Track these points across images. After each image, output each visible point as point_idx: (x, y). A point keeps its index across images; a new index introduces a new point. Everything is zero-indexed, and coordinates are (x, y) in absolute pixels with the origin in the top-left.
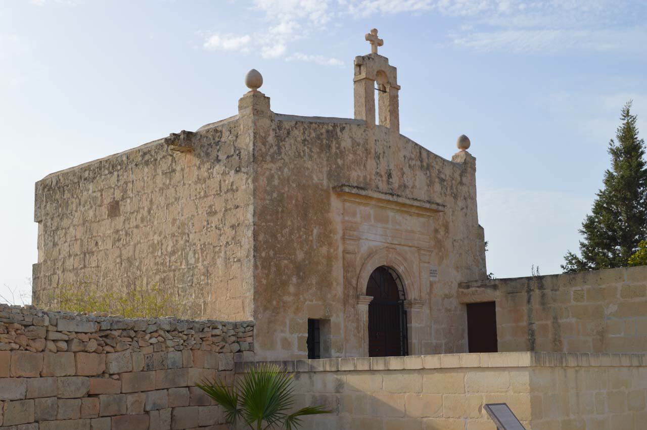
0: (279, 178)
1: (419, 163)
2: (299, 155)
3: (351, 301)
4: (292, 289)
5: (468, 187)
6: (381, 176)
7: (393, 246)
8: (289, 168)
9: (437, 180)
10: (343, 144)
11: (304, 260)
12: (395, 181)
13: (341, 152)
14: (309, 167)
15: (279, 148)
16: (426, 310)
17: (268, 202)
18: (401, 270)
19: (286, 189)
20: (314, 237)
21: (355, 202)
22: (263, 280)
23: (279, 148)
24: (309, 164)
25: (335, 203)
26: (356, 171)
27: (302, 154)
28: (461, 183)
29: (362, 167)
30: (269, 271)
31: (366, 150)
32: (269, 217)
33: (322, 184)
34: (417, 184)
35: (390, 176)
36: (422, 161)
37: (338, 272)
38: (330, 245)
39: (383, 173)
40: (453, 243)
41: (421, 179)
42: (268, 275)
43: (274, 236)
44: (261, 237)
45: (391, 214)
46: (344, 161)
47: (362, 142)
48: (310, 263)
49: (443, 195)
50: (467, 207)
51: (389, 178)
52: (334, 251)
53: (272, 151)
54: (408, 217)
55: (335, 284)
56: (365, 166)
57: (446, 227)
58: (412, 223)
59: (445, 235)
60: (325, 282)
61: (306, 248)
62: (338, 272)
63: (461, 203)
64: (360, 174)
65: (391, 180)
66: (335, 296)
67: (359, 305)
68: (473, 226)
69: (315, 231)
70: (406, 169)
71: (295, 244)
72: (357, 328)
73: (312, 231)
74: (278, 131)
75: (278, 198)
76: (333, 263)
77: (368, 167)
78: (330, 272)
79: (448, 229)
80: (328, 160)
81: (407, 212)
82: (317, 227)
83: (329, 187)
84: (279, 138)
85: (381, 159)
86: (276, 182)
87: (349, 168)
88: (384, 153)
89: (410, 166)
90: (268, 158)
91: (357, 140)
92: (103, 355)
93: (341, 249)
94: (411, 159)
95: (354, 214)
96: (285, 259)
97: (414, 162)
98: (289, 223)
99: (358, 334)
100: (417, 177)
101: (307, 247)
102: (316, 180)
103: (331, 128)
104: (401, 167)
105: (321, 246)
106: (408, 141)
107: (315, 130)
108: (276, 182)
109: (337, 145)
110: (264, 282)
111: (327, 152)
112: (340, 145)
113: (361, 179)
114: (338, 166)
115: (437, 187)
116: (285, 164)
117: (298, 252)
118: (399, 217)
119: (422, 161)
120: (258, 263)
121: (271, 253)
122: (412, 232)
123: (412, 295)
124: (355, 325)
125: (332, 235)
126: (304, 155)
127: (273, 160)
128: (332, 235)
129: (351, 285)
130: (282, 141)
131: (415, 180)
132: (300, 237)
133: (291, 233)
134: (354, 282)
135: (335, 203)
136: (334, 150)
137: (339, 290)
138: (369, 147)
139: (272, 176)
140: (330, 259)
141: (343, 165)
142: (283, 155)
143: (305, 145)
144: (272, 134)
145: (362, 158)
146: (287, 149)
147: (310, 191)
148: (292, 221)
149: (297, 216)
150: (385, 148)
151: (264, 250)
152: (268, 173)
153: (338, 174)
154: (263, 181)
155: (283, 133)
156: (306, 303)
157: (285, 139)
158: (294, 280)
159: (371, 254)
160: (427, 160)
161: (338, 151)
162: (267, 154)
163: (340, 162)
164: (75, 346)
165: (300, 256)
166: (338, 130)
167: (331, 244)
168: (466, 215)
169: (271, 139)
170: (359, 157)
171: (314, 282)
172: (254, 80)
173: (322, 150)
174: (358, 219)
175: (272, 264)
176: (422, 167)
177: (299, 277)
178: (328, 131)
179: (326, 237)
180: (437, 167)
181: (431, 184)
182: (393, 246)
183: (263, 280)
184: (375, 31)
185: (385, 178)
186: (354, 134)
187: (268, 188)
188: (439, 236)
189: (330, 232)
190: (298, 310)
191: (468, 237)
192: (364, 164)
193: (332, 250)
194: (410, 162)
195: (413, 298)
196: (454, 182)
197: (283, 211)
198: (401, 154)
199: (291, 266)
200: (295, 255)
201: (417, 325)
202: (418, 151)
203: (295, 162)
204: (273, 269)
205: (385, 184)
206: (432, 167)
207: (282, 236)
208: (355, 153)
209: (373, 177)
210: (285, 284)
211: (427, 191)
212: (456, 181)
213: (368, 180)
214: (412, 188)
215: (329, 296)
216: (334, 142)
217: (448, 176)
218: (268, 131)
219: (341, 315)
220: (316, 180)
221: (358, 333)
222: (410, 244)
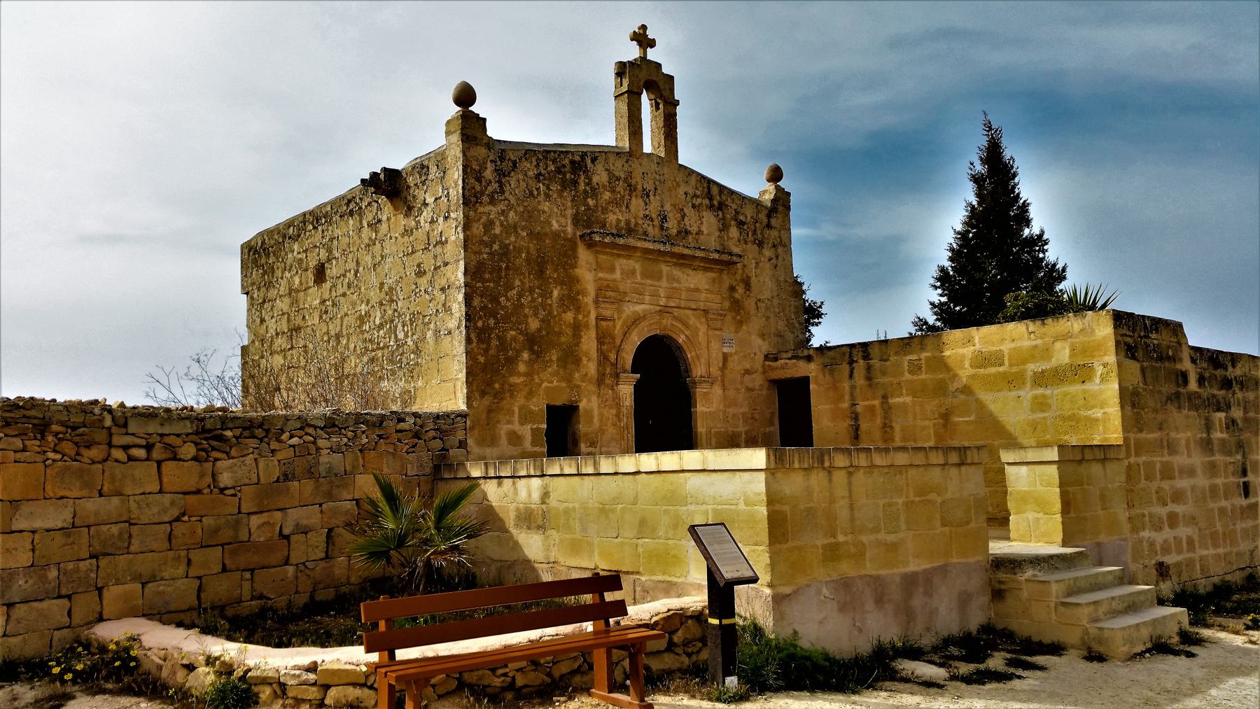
0: (502, 225)
1: (707, 202)
2: (531, 193)
4: (522, 368)
5: (779, 231)
6: (652, 220)
7: (670, 310)
8: (516, 212)
9: (733, 223)
10: (595, 179)
11: (539, 330)
12: (672, 225)
13: (593, 189)
14: (546, 209)
16: (717, 390)
17: (485, 256)
18: (681, 339)
19: (513, 239)
20: (554, 301)
21: (612, 254)
22: (479, 357)
24: (546, 206)
25: (584, 254)
26: (614, 213)
27: (536, 193)
28: (769, 226)
29: (624, 209)
30: (489, 344)
31: (630, 185)
32: (487, 276)
33: (564, 232)
34: (704, 229)
35: (664, 219)
36: (711, 199)
38: (578, 309)
39: (654, 216)
40: (756, 303)
41: (709, 223)
42: (486, 351)
43: (495, 300)
44: (476, 302)
45: (665, 269)
46: (597, 201)
47: (623, 176)
48: (548, 333)
49: (742, 242)
50: (777, 257)
51: (663, 222)
52: (583, 318)
54: (691, 272)
55: (585, 360)
56: (627, 207)
57: (747, 283)
58: (697, 280)
59: (745, 293)
60: (571, 358)
61: (542, 314)
62: (589, 343)
63: (768, 252)
64: (620, 218)
65: (666, 225)
66: (586, 375)
67: (620, 387)
68: (786, 281)
69: (556, 293)
70: (689, 211)
71: (527, 311)
72: (618, 415)
74: (499, 163)
75: (500, 251)
76: (583, 333)
77: (632, 208)
78: (577, 344)
79: (750, 286)
80: (573, 200)
82: (559, 288)
83: (574, 234)
84: (501, 174)
85: (652, 197)
86: (497, 230)
87: (605, 210)
88: (656, 189)
90: (485, 199)
91: (617, 174)
92: (209, 465)
93: (593, 316)
94: (695, 196)
95: (612, 270)
96: (511, 329)
97: (699, 201)
98: (517, 283)
99: (618, 423)
100: (704, 220)
101: (543, 313)
102: (555, 226)
103: (577, 158)
104: (681, 207)
105: (565, 312)
106: (691, 172)
107: (554, 161)
108: (497, 230)
109: (587, 181)
110: (482, 359)
111: (571, 191)
112: (591, 180)
113: (623, 224)
114: (589, 208)
115: (734, 232)
116: (510, 207)
117: (530, 320)
118: (677, 272)
119: (711, 199)
120: (473, 336)
121: (492, 322)
122: (697, 290)
123: (698, 371)
124: (614, 411)
125: (580, 297)
126: (539, 194)
127: (492, 202)
128: (580, 297)
129: (608, 360)
130: (504, 176)
131: (702, 223)
132: (533, 300)
133: (520, 295)
134: (612, 357)
135: (584, 254)
136: (582, 187)
137: (591, 368)
138: (633, 182)
140: (577, 328)
141: (596, 206)
142: (507, 194)
143: (539, 181)
144: (490, 167)
145: (623, 197)
146: (512, 186)
147: (547, 242)
148: (520, 280)
149: (529, 274)
150: (657, 183)
151: (480, 318)
152: (484, 218)
153: (589, 218)
154: (477, 229)
155: (506, 166)
156: (544, 385)
157: (509, 173)
158: (526, 355)
161: (588, 188)
162: (482, 193)
163: (591, 202)
164: (157, 454)
165: (534, 324)
166: (589, 161)
167: (579, 308)
168: (776, 266)
169: (489, 173)
170: (619, 196)
171: (554, 358)
172: (465, 96)
173: (564, 188)
174: (617, 275)
175: (492, 336)
176: (711, 207)
177: (531, 350)
178: (572, 162)
179: (572, 300)
180: (734, 206)
181: (724, 228)
182: (670, 310)
183: (479, 357)
184: (644, 27)
185: (656, 223)
186: (611, 165)
187: (485, 238)
188: (737, 296)
189: (578, 293)
190: (531, 394)
191: (778, 295)
192: (627, 205)
193: (580, 317)
194: (694, 202)
195: (699, 374)
196: (758, 225)
197: (507, 268)
198: (681, 191)
199: (521, 338)
200: (527, 324)
201: (704, 409)
202: (705, 185)
203: (526, 204)
204: (495, 343)
205: (657, 230)
206: (726, 206)
207: (508, 300)
208: (613, 191)
209: (641, 222)
210: (511, 361)
211: (719, 237)
212: (761, 223)
213: (632, 225)
214: (697, 234)
215: (577, 375)
216: (582, 177)
217: (749, 218)
218: (486, 163)
219: (594, 398)
220: (555, 226)
221: (619, 421)
222: (694, 307)
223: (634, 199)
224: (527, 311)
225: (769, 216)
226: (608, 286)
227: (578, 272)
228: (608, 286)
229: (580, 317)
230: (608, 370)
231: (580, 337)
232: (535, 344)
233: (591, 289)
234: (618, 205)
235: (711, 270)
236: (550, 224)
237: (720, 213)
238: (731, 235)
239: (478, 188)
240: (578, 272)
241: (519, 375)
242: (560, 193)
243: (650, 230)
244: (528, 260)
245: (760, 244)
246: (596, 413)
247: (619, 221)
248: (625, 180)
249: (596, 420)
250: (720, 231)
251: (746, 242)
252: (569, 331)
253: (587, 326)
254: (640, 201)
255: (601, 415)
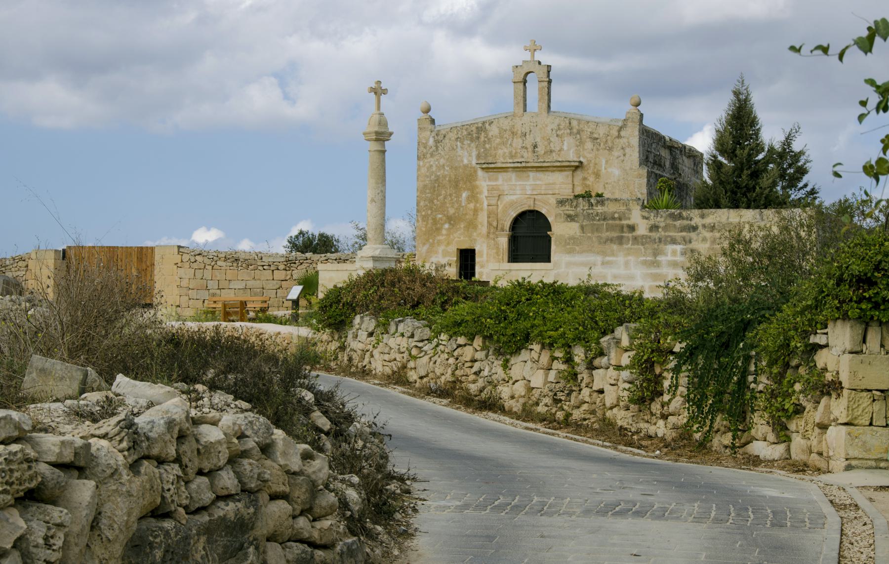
0: (436, 166)
1: (568, 131)
2: (453, 149)
3: (492, 236)
4: (444, 232)
5: (628, 139)
6: (526, 148)
9: (588, 140)
10: (490, 134)
11: (454, 214)
12: (541, 150)
15: (437, 147)
23: (437, 147)
28: (619, 137)
30: (427, 223)
31: (513, 133)
32: (428, 191)
35: (535, 146)
36: (571, 129)
37: (483, 218)
38: (477, 202)
39: (528, 146)
44: (422, 204)
45: (532, 174)
50: (624, 155)
53: (431, 150)
55: (480, 226)
60: (472, 225)
61: (456, 205)
62: (483, 218)
63: (616, 153)
65: (536, 149)
67: (499, 239)
68: (631, 169)
70: (554, 139)
71: (448, 205)
72: (497, 253)
73: (461, 195)
79: (599, 176)
81: (547, 171)
86: (434, 169)
87: (496, 149)
89: (557, 136)
93: (486, 203)
98: (443, 192)
102: (466, 161)
103: (480, 125)
108: (434, 169)
110: (424, 229)
112: (487, 135)
114: (486, 149)
115: (589, 145)
117: (449, 209)
118: (540, 175)
119: (571, 129)
121: (429, 212)
124: (495, 251)
127: (432, 155)
132: (452, 200)
133: (445, 198)
136: (482, 139)
137: (484, 230)
138: (515, 130)
139: (431, 166)
140: (476, 211)
141: (490, 148)
153: (486, 154)
154: (424, 170)
155: (440, 138)
158: (447, 226)
159: (512, 204)
160: (577, 127)
165: (451, 211)
166: (487, 125)
171: (462, 226)
177: (450, 223)
178: (477, 128)
180: (590, 130)
181: (581, 143)
185: (530, 149)
187: (428, 174)
189: (477, 193)
190: (448, 244)
193: (478, 205)
194: (558, 132)
196: (609, 138)
197: (439, 186)
198: (549, 129)
200: (448, 211)
202: (568, 122)
205: (530, 154)
206: (583, 131)
208: (501, 137)
209: (519, 151)
213: (513, 154)
215: (475, 234)
216: (483, 134)
217: (601, 135)
223: (515, 140)
224: (448, 205)
225: (619, 131)
226: (493, 188)
227: (478, 183)
228: (493, 188)
229: (478, 205)
230: (492, 231)
231: (478, 215)
232: (451, 220)
233: (486, 193)
234: (504, 143)
235: (565, 170)
236: (462, 161)
237: (578, 136)
238: (586, 147)
239: (425, 151)
240: (478, 183)
241: (442, 235)
242: (469, 145)
243: (525, 155)
244: (450, 181)
245: (610, 149)
246: (485, 252)
247: (505, 153)
248: (510, 130)
249: (485, 256)
250: (577, 146)
251: (598, 150)
252: (471, 213)
253: (482, 209)
254: (520, 140)
255: (487, 252)
